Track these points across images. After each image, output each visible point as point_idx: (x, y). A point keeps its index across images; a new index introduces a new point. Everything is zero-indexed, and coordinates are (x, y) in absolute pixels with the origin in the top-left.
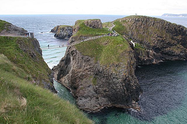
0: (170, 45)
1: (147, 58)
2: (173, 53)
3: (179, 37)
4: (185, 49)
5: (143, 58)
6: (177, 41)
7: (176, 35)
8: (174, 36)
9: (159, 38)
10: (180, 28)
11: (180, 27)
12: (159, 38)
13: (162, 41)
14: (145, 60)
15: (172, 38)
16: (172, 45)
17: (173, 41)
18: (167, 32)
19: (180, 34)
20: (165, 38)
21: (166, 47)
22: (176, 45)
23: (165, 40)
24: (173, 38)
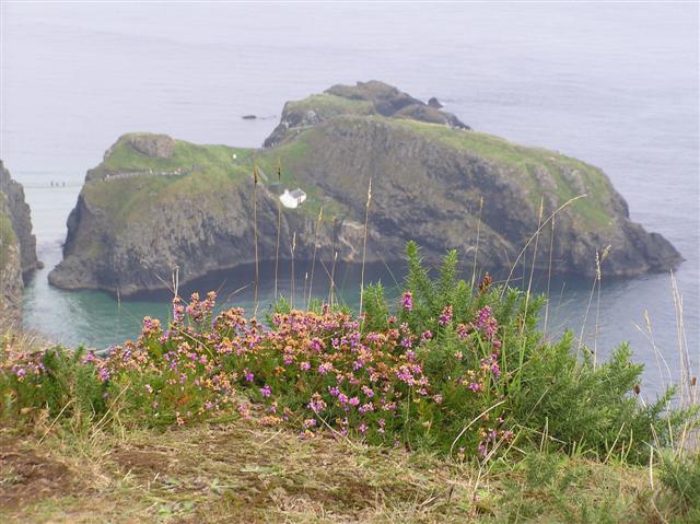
0: (432, 213)
1: (328, 242)
2: (442, 241)
3: (473, 194)
4: (493, 233)
5: (310, 240)
6: (464, 204)
7: (465, 187)
8: (458, 188)
9: (395, 192)
10: (475, 165)
11: (475, 162)
12: (395, 192)
13: (409, 200)
14: (319, 246)
15: (449, 196)
16: (444, 218)
17: (451, 205)
18: (429, 175)
19: (476, 184)
20: (415, 193)
21: (419, 222)
22: (460, 218)
23: (416, 201)
24: (452, 195)
